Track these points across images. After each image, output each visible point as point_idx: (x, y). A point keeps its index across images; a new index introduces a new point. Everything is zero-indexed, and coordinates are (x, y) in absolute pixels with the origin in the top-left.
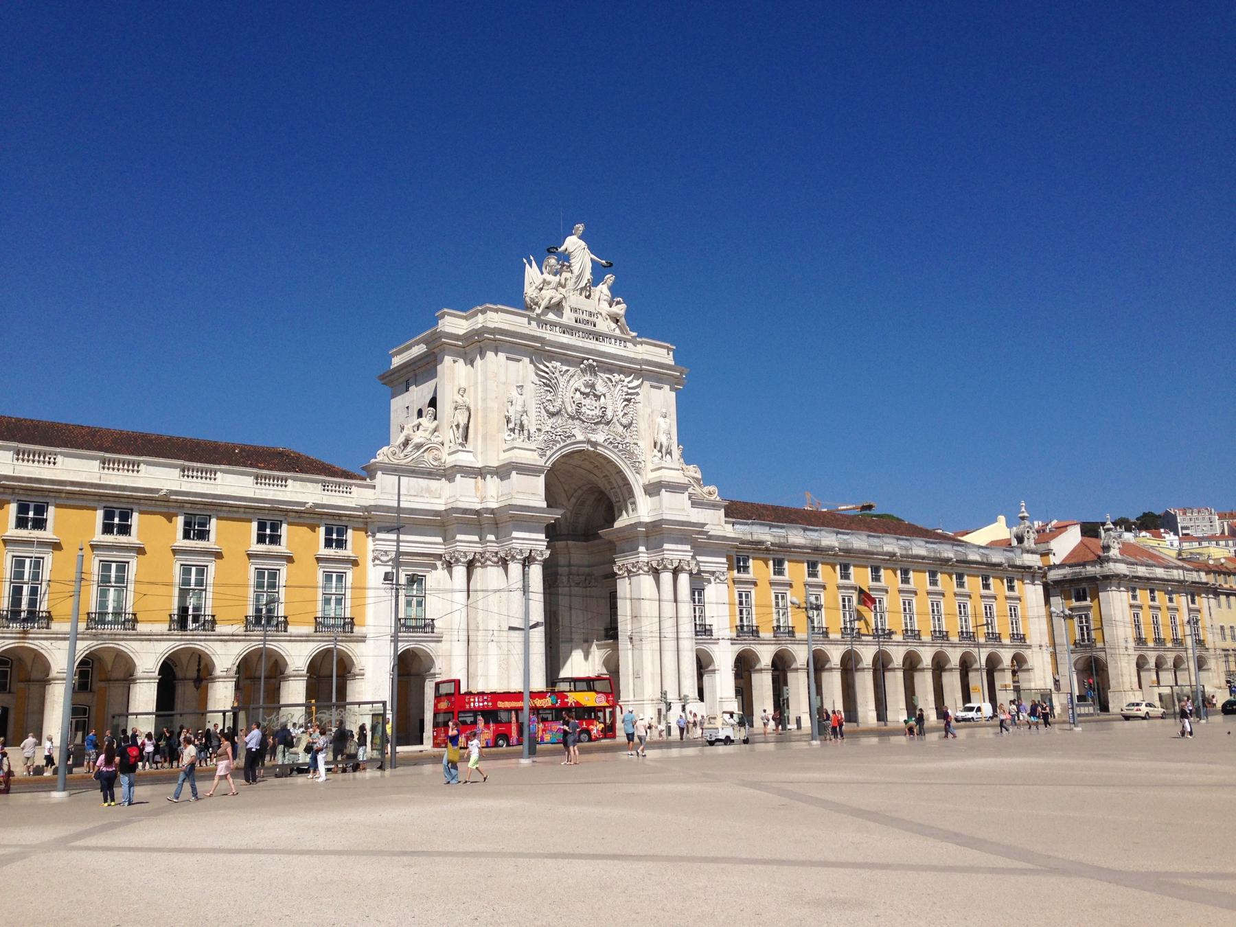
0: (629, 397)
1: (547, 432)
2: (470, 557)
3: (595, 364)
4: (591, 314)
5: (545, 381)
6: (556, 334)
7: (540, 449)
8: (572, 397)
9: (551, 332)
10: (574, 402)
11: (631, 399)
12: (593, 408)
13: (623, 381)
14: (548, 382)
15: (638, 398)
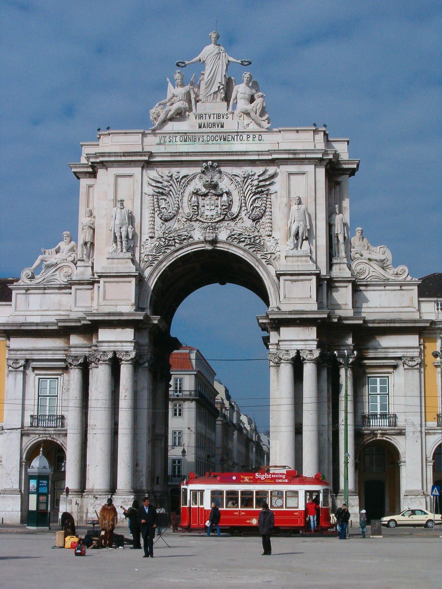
0: (260, 189)
1: (160, 238)
2: (81, 361)
3: (215, 164)
4: (219, 116)
5: (157, 190)
6: (177, 143)
7: (151, 255)
8: (190, 201)
9: (171, 143)
10: (191, 205)
11: (264, 191)
12: (213, 207)
13: (252, 175)
14: (161, 190)
15: (272, 188)
